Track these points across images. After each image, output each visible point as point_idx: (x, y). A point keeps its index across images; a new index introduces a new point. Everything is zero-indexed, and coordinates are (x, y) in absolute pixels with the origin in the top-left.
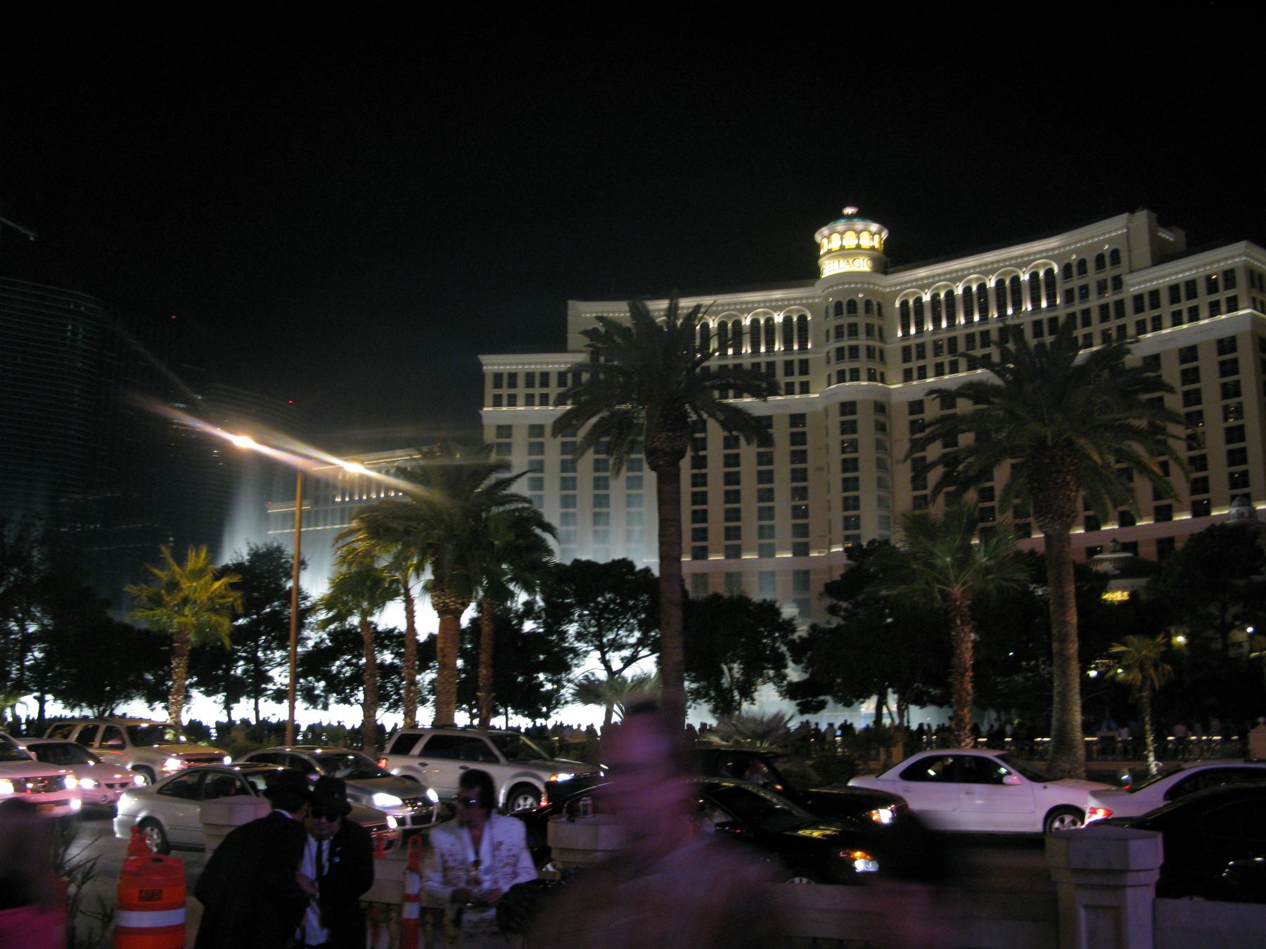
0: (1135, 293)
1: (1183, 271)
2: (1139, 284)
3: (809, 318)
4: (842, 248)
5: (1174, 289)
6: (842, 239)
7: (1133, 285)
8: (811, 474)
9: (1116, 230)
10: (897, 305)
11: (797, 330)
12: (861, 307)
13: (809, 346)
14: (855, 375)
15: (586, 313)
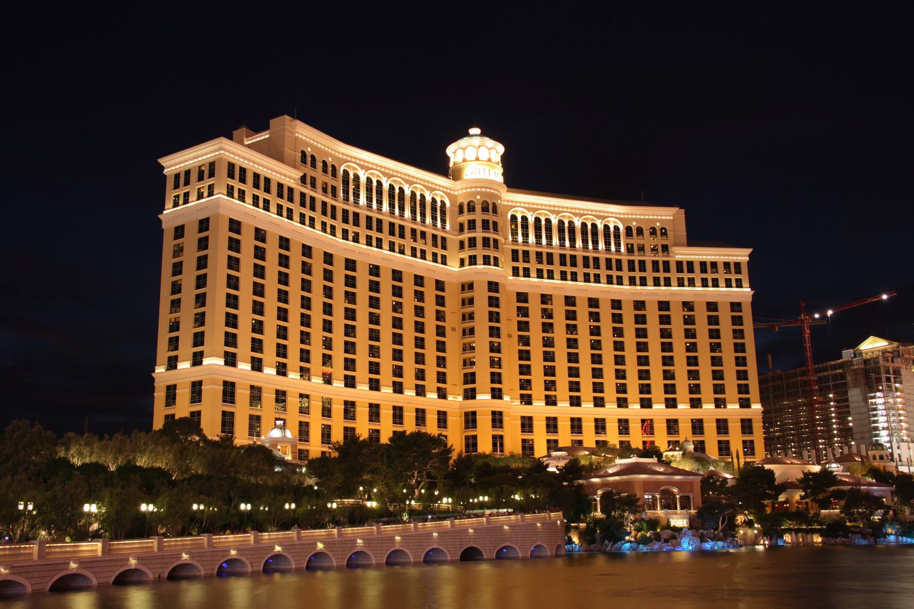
0: (677, 260)
1: (711, 255)
2: (682, 254)
3: (448, 204)
4: (490, 160)
5: (703, 264)
6: (490, 153)
7: (678, 254)
8: (448, 331)
9: (666, 216)
10: (509, 217)
11: (438, 210)
12: (499, 210)
13: (448, 227)
14: (496, 264)
15: (298, 133)
